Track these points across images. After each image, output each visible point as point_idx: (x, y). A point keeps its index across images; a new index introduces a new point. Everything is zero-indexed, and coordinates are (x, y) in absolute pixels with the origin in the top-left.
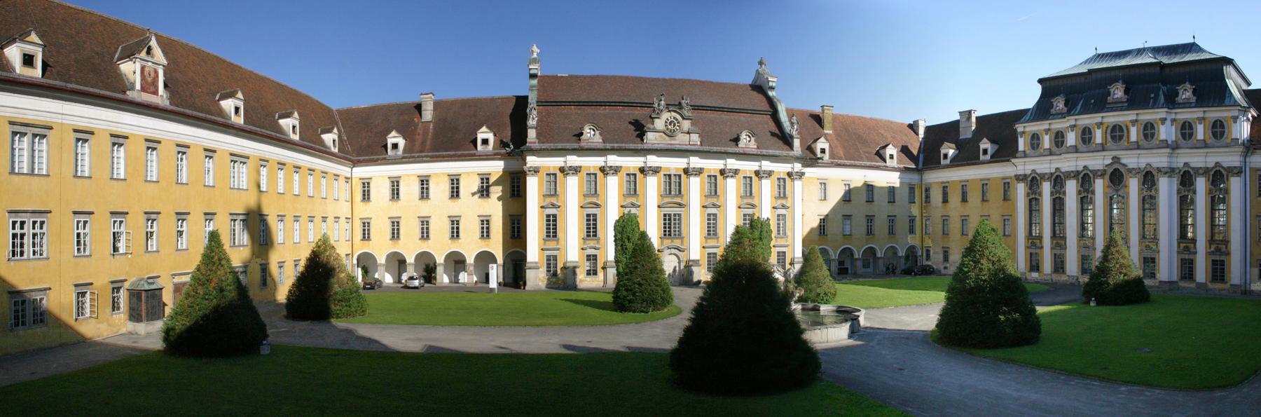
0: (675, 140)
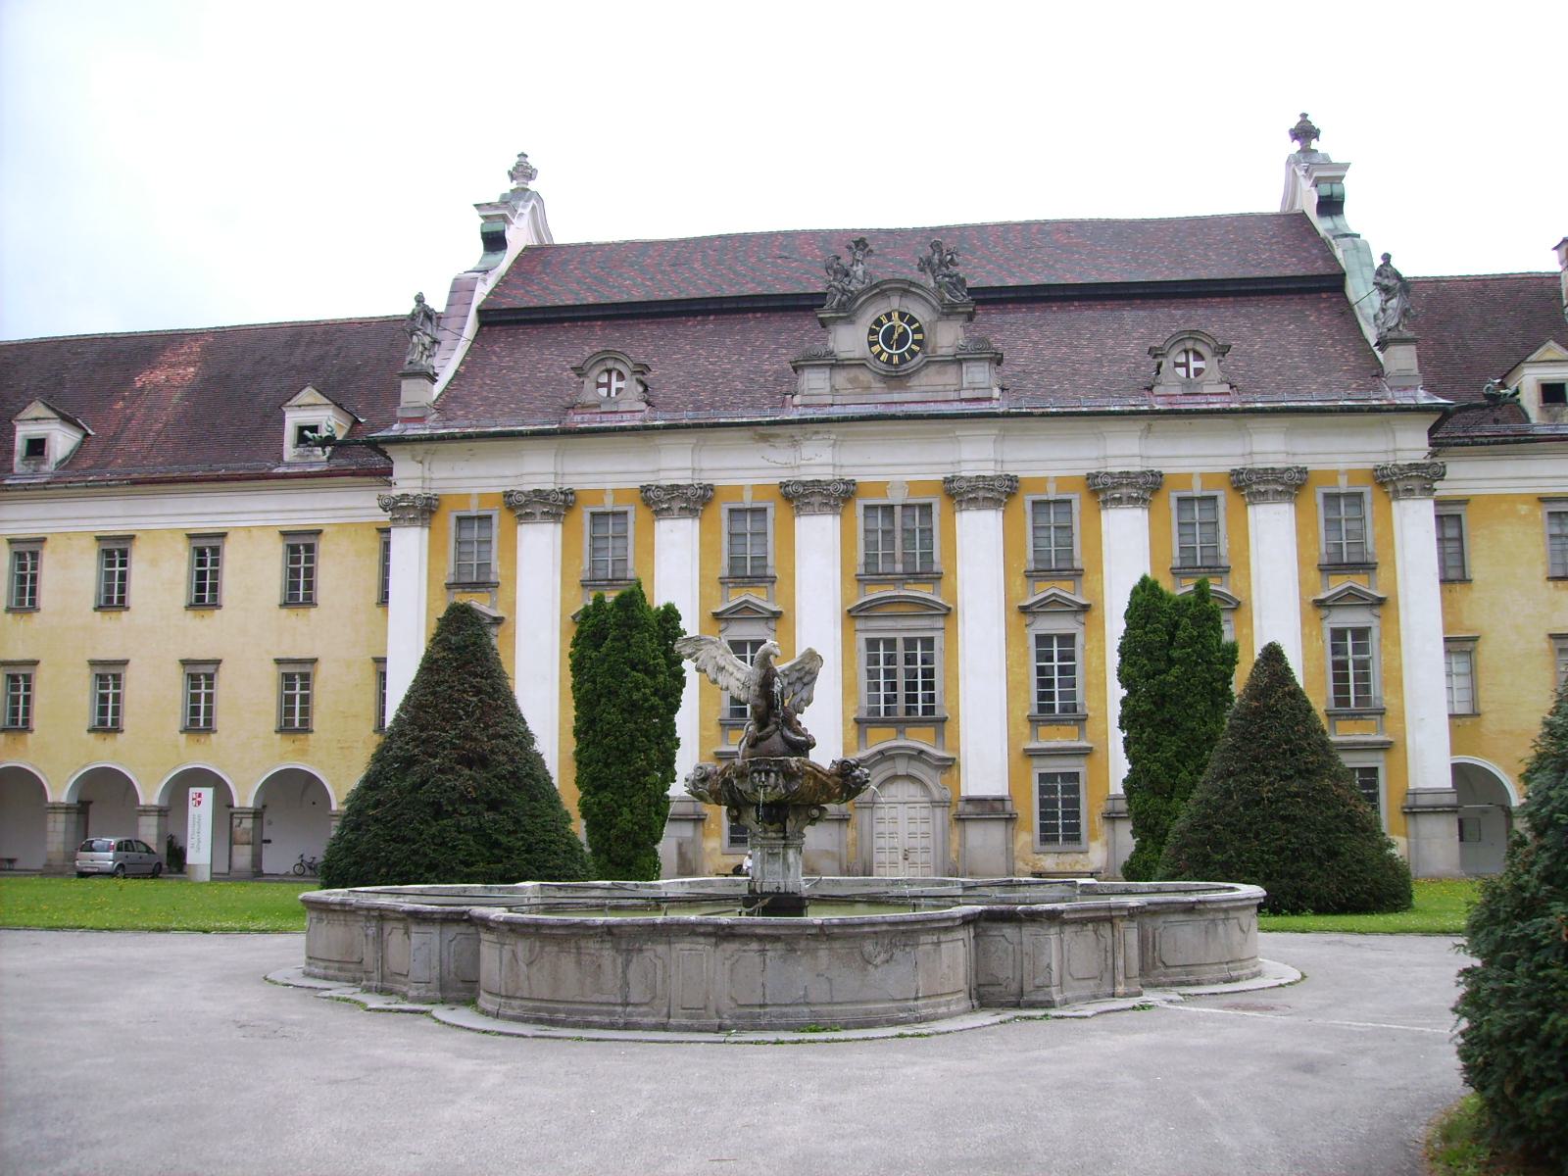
0: (907, 389)
